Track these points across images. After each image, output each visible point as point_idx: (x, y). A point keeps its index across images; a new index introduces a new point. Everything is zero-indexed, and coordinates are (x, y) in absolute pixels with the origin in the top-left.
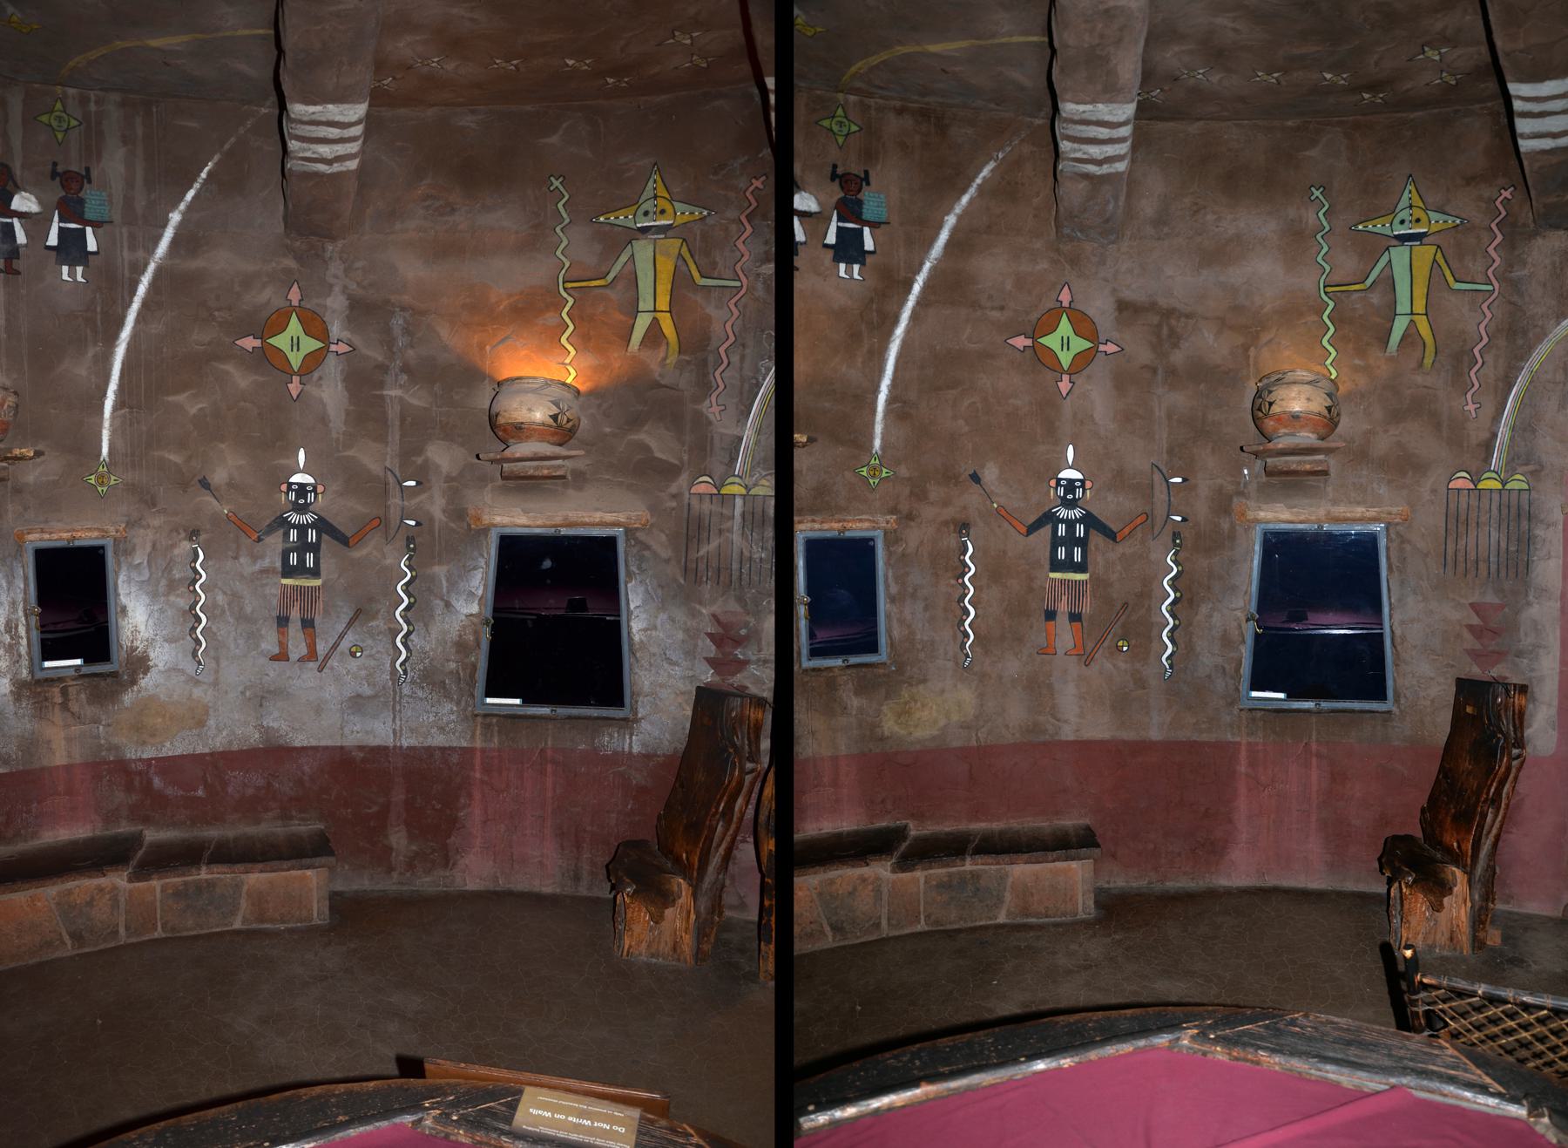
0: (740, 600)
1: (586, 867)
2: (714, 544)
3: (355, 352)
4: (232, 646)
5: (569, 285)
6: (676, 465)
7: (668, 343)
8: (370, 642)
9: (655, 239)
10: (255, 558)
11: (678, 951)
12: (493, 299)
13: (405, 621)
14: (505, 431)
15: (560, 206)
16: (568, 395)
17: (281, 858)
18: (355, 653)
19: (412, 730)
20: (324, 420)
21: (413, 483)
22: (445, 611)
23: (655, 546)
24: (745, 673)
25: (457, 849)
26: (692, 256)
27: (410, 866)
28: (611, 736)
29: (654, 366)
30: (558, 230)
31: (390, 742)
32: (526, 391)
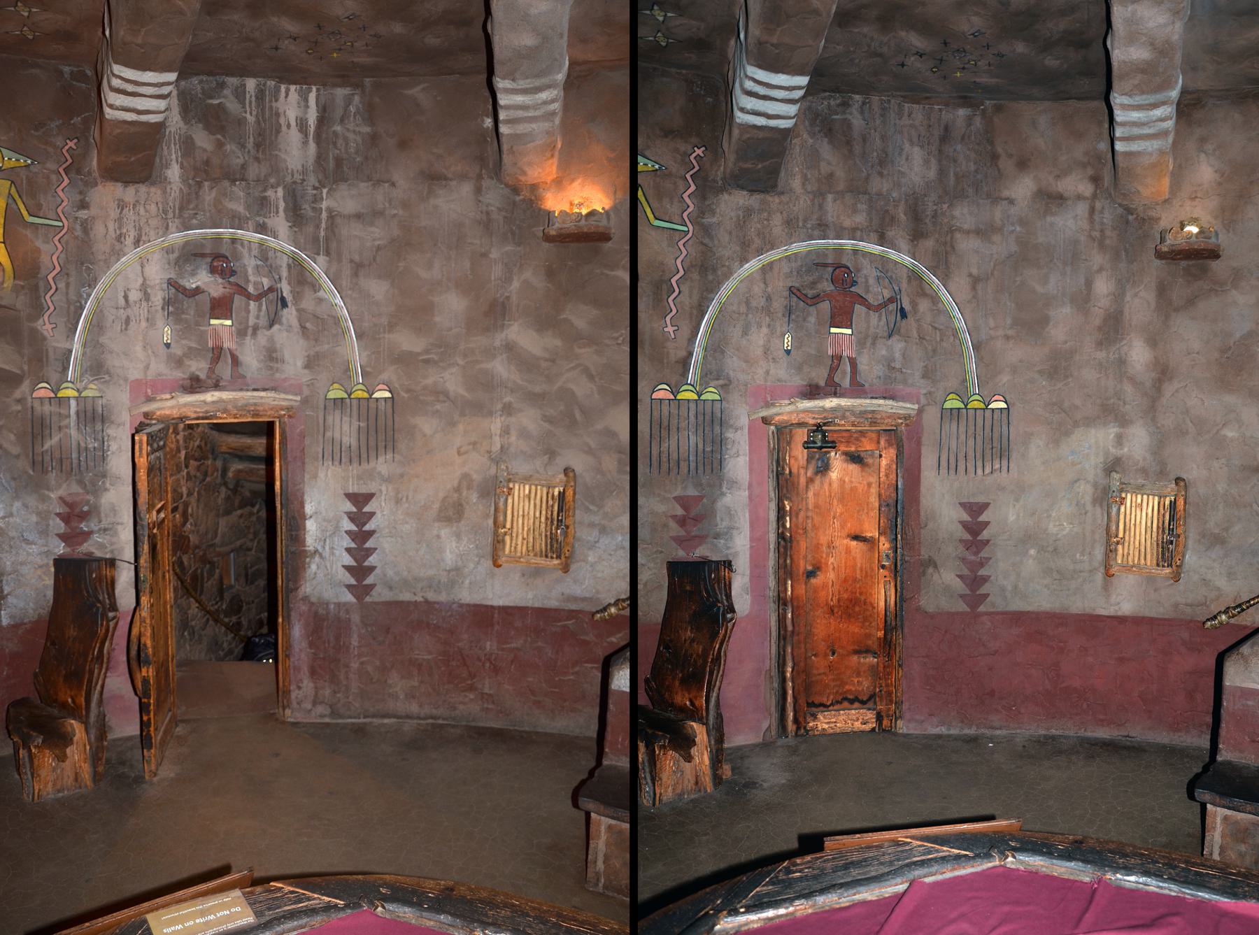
0: (81, 482)
2: (56, 439)
6: (17, 375)
11: (79, 780)
23: (6, 445)
24: (90, 542)
26: (20, 196)
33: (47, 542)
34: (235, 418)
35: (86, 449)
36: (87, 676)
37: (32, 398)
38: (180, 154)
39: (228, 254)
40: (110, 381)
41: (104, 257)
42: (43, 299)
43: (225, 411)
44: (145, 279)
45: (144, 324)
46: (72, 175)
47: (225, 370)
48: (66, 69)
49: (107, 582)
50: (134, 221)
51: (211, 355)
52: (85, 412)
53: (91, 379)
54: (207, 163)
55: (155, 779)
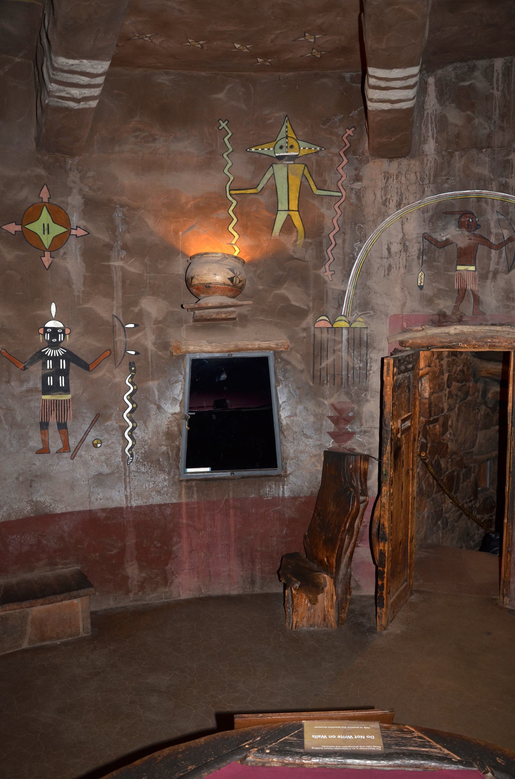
0: (348, 394)
1: (258, 575)
3: (90, 235)
4: (8, 446)
5: (233, 192)
7: (297, 231)
8: (106, 436)
9: (288, 164)
10: (22, 382)
11: (327, 621)
12: (183, 200)
13: (130, 420)
14: (198, 289)
15: (226, 139)
16: (239, 265)
17: (55, 593)
18: (97, 444)
19: (138, 495)
20: (68, 282)
21: (132, 326)
22: (158, 412)
23: (294, 362)
24: (353, 440)
25: (173, 572)
26: (311, 175)
27: (141, 587)
28: (271, 487)
29: (290, 246)
30: (225, 155)
31: (124, 504)
32: (212, 262)
33: (320, 437)
34: (474, 348)
35: (353, 368)
36: (339, 543)
37: (315, 328)
38: (435, 131)
39: (473, 211)
40: (374, 315)
41: (372, 219)
42: (325, 252)
43: (466, 341)
44: (404, 235)
45: (402, 270)
46: (350, 156)
47: (467, 307)
48: (348, 75)
49: (360, 472)
50: (397, 188)
51: (457, 295)
52: (354, 339)
53: (360, 314)
54: (458, 136)
55: (385, 632)
